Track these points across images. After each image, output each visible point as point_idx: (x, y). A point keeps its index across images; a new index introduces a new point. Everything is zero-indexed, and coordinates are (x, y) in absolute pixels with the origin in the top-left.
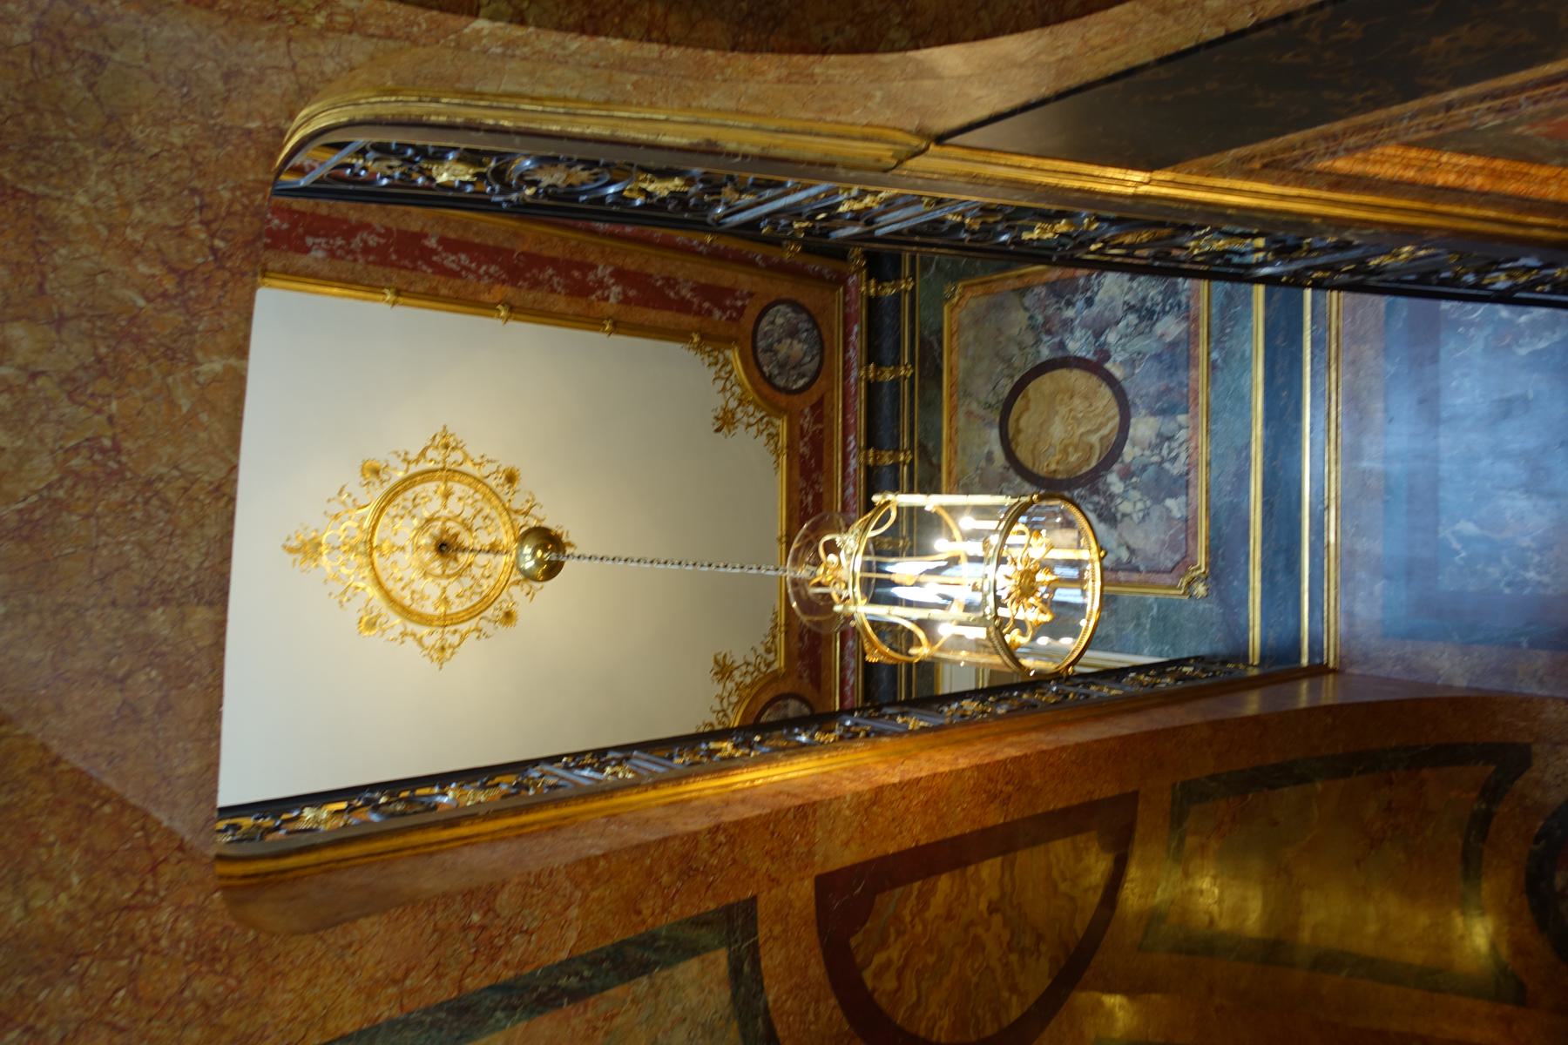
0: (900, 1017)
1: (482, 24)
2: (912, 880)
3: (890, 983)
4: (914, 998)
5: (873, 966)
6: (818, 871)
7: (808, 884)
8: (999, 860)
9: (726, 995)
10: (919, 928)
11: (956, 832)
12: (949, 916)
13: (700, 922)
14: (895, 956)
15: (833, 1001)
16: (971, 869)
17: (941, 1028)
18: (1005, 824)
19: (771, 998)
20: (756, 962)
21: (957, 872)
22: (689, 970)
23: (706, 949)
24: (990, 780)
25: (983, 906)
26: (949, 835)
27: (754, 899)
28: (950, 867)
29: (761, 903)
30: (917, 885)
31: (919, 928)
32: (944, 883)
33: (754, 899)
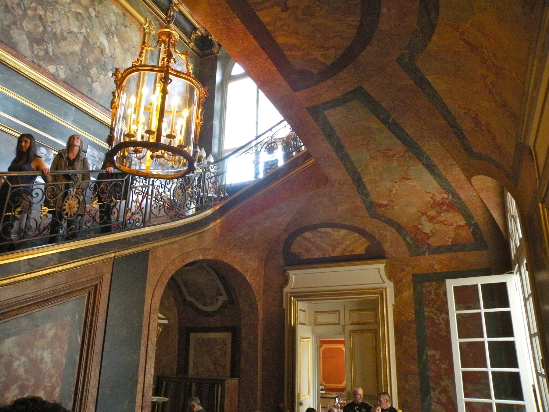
0: (347, 44)
1: (201, 258)
2: (284, 55)
3: (332, 52)
4: (339, 39)
5: (325, 61)
6: (292, 92)
7: (297, 94)
8: (257, 13)
9: (339, 108)
10: (305, 46)
11: (255, 42)
12: (296, 32)
13: (317, 120)
14: (320, 53)
15: (341, 74)
16: (270, 28)
17: (353, 21)
18: (238, 16)
19: (340, 95)
20: (328, 102)
21: (273, 35)
22: (331, 120)
23: (325, 116)
24: (222, 34)
25: (285, 15)
26: (258, 45)
27: (307, 108)
28: (273, 40)
29: (307, 106)
30: (285, 52)
31: (305, 46)
32: (280, 40)
33: (307, 108)
